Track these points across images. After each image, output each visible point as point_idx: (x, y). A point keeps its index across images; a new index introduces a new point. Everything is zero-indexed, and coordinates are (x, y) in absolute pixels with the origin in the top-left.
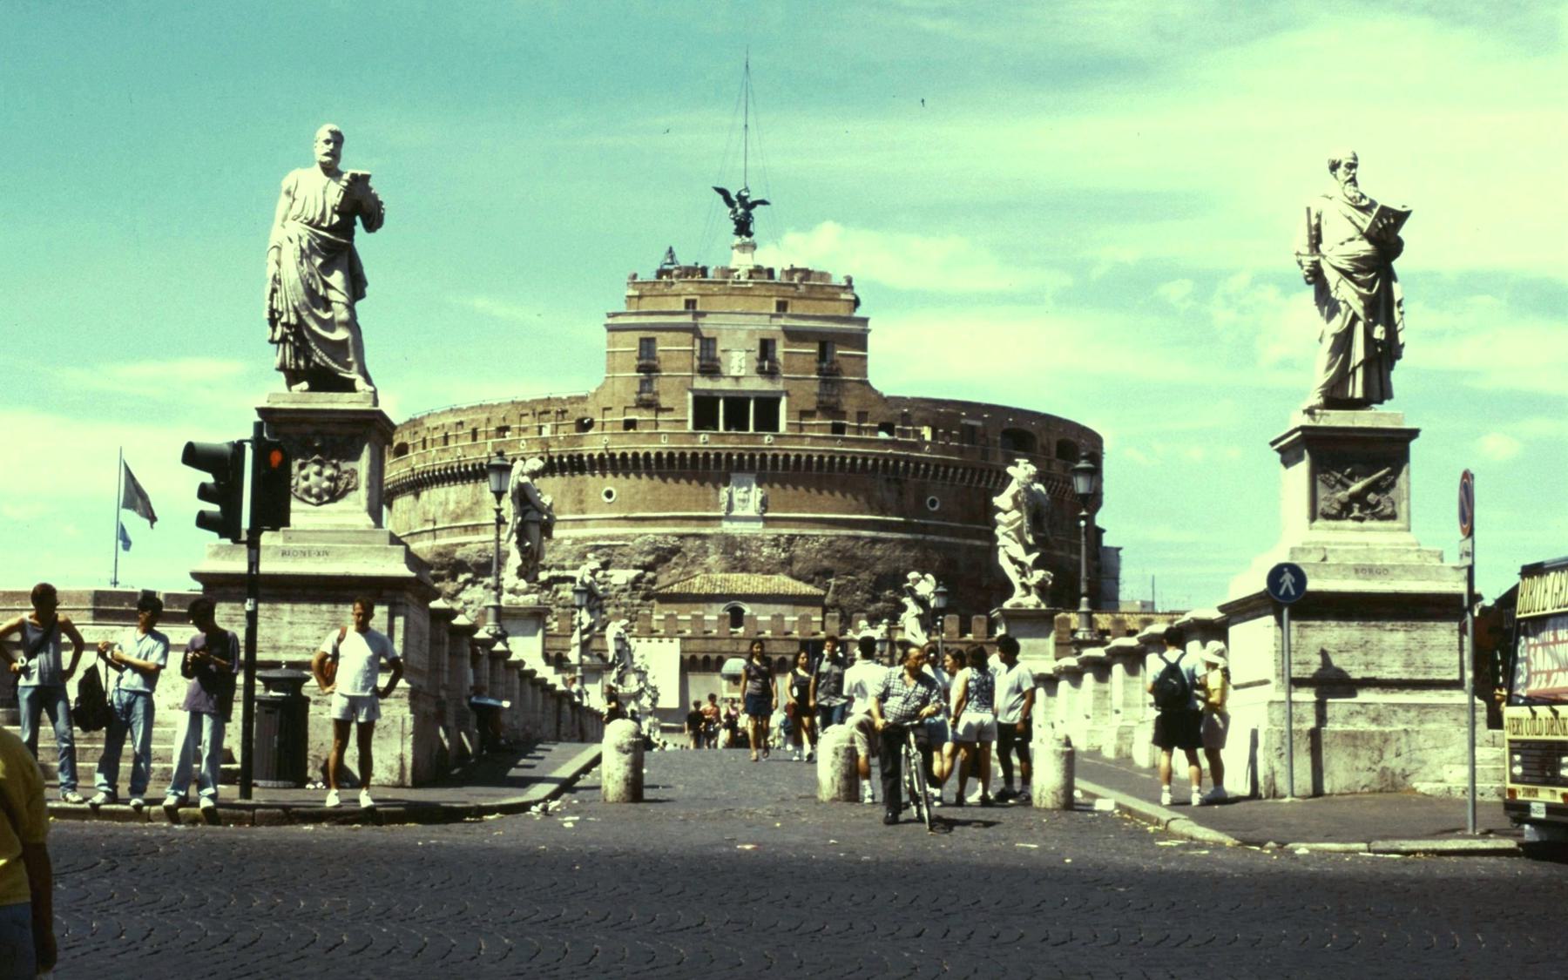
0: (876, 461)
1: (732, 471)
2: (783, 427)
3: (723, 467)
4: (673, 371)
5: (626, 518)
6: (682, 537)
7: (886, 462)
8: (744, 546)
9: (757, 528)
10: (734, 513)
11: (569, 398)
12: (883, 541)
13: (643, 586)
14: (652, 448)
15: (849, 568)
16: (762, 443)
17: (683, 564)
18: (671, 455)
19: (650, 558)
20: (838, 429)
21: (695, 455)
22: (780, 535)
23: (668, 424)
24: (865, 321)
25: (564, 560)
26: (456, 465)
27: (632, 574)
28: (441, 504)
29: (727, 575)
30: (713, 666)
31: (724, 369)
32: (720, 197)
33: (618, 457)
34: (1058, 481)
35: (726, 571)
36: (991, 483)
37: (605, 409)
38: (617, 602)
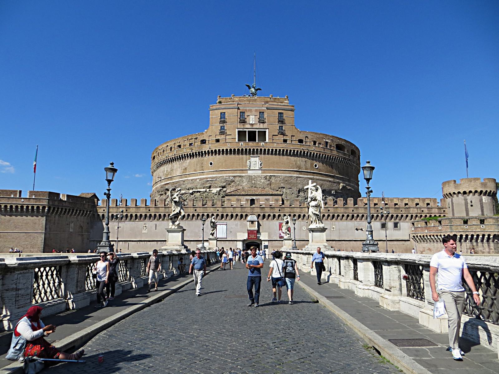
0: (298, 151)
1: (251, 155)
4: (231, 122)
5: (216, 171)
6: (234, 177)
8: (255, 179)
10: (251, 169)
12: (300, 177)
13: (222, 193)
15: (290, 186)
17: (235, 186)
18: (231, 150)
19: (225, 184)
20: (285, 141)
21: (238, 150)
23: (230, 140)
24: (293, 106)
25: (197, 186)
26: (166, 159)
27: (218, 189)
29: (250, 189)
30: (244, 217)
33: (214, 151)
34: (352, 162)
37: (209, 136)
38: (213, 199)
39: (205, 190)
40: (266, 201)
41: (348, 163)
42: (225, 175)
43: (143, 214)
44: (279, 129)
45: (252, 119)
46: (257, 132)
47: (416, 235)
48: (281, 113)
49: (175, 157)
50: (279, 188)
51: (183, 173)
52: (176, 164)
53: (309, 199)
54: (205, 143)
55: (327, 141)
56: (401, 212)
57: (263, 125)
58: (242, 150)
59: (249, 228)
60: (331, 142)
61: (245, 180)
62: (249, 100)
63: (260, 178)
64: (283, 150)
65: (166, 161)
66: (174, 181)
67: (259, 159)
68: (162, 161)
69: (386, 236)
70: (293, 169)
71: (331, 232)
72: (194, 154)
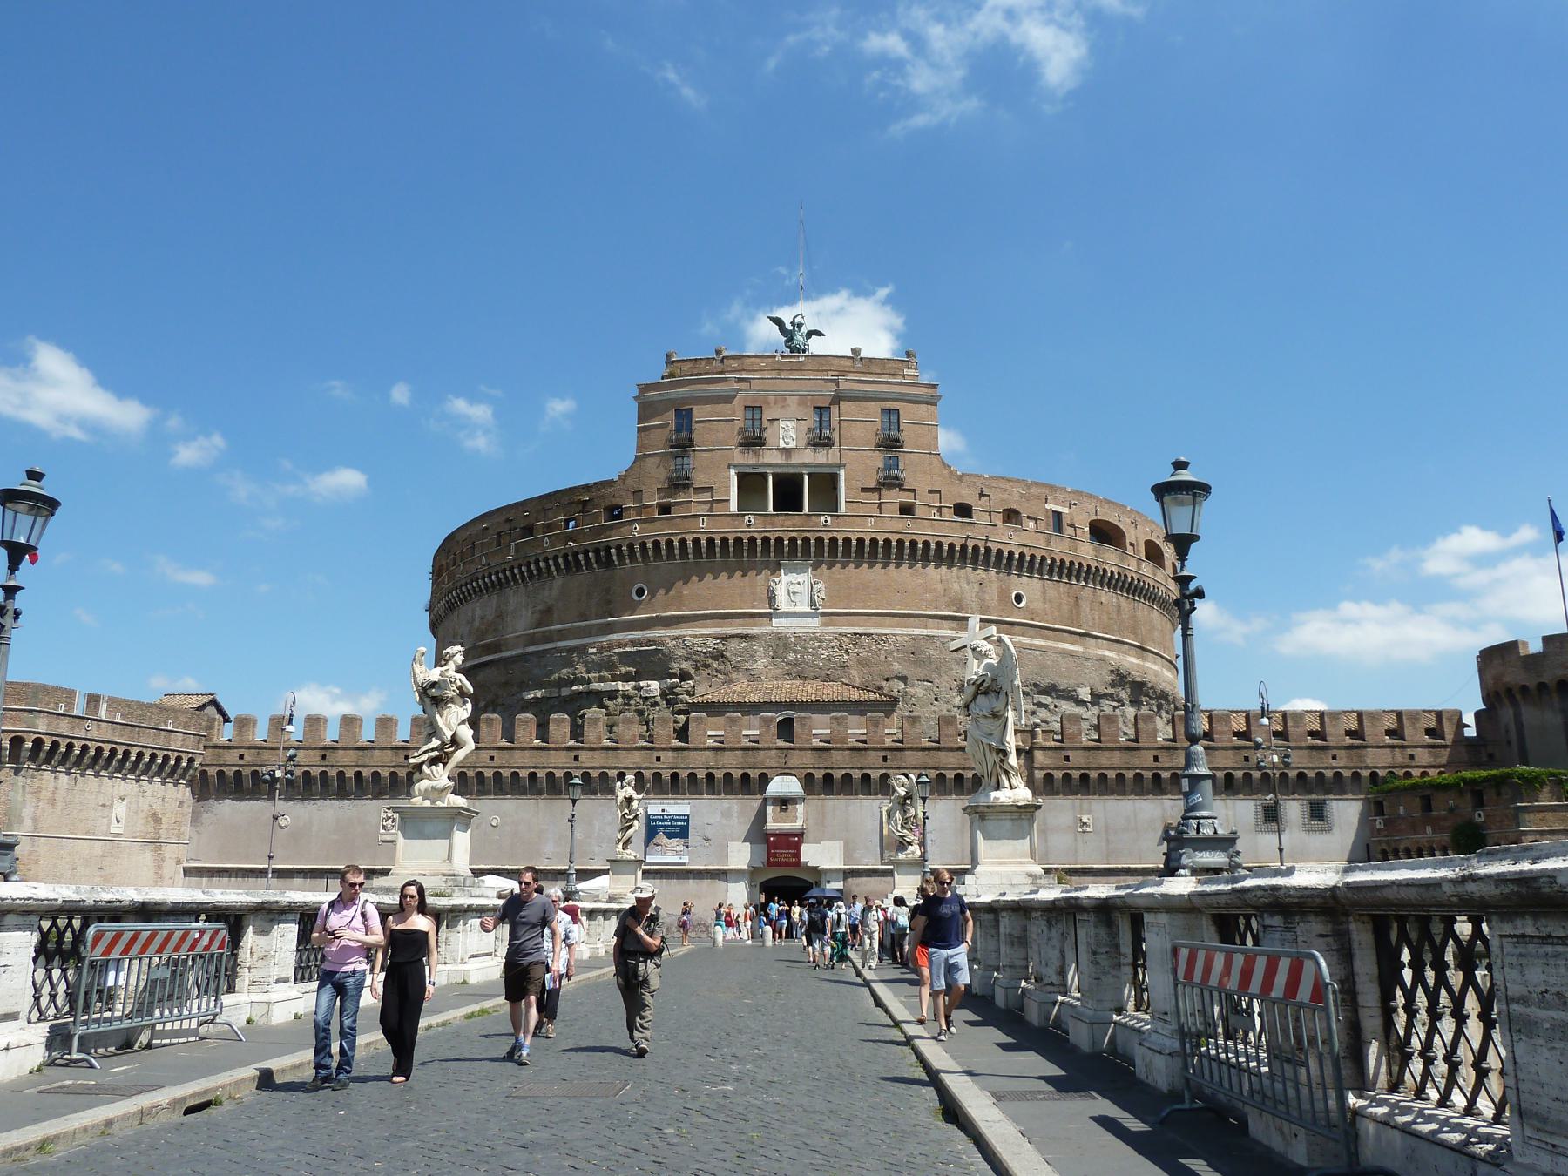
1: (783, 558)
3: (772, 554)
7: (964, 547)
9: (813, 625)
11: (595, 484)
14: (689, 532)
15: (923, 673)
16: (818, 524)
18: (710, 541)
19: (685, 665)
20: (906, 510)
21: (738, 541)
22: (840, 634)
24: (934, 386)
26: (480, 576)
28: (468, 622)
30: (755, 786)
31: (770, 443)
33: (649, 546)
35: (778, 679)
40: (835, 724)
42: (690, 632)
43: (385, 773)
44: (881, 465)
45: (788, 433)
46: (806, 478)
47: (1393, 845)
48: (889, 411)
49: (512, 569)
50: (887, 680)
54: (620, 513)
55: (1058, 509)
56: (1334, 763)
57: (828, 454)
59: (771, 825)
60: (1070, 513)
61: (760, 650)
62: (777, 367)
65: (480, 582)
66: (508, 654)
68: (466, 584)
69: (1281, 850)
70: (936, 608)
71: (1076, 840)
72: (581, 557)
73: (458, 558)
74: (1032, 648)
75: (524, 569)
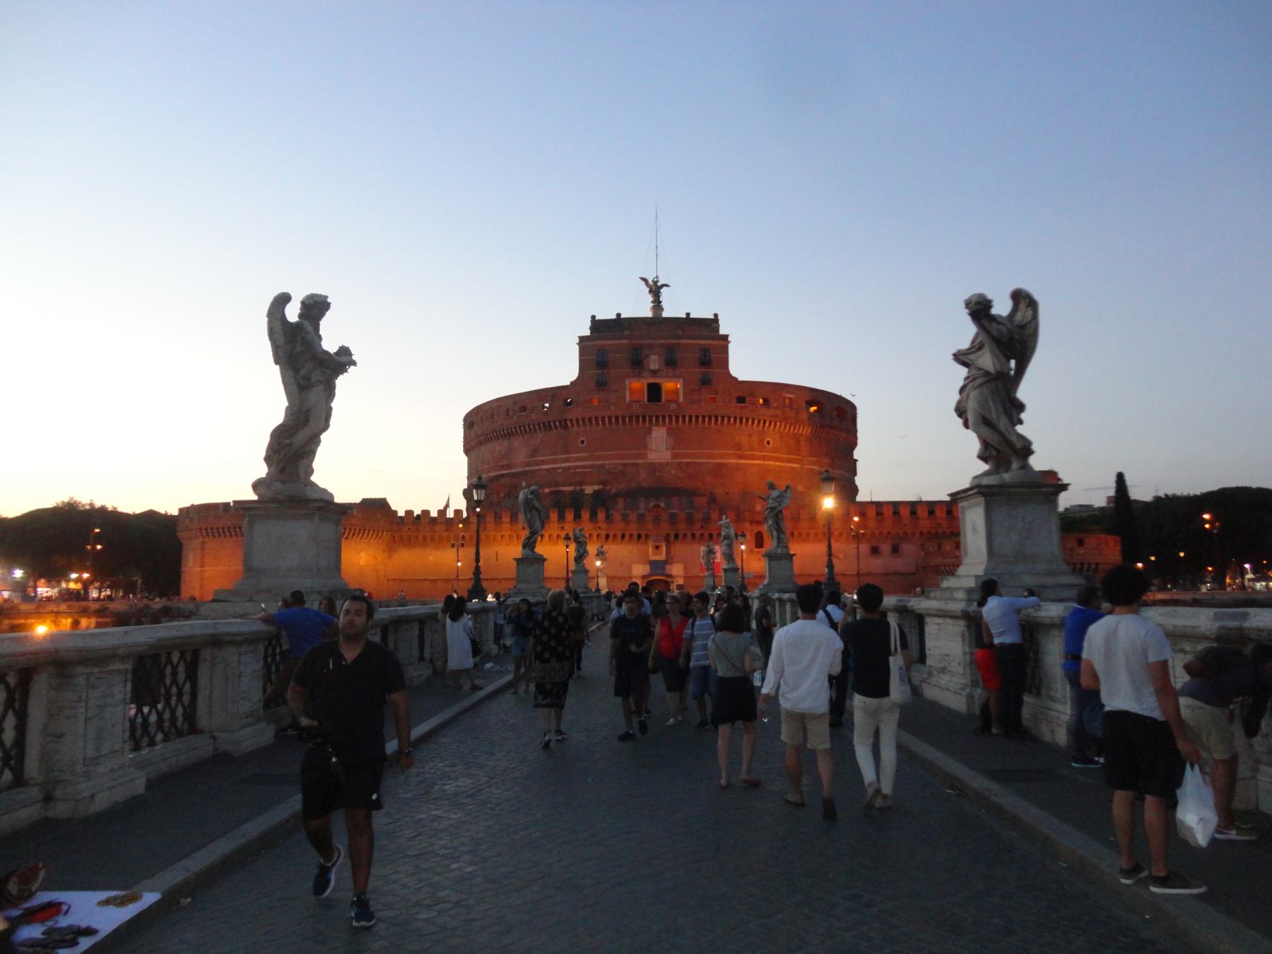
0: (735, 419)
2: (681, 399)
6: (625, 465)
18: (617, 418)
20: (714, 400)
22: (681, 463)
27: (596, 487)
32: (643, 283)
33: (587, 420)
36: (800, 432)
39: (571, 488)
41: (830, 433)
42: (607, 462)
45: (654, 362)
49: (515, 428)
51: (531, 456)
52: (517, 442)
53: (722, 538)
58: (637, 417)
59: (652, 558)
63: (670, 467)
64: (710, 417)
65: (498, 433)
67: (668, 433)
72: (552, 424)
73: (484, 419)
74: (774, 466)
75: (522, 428)
